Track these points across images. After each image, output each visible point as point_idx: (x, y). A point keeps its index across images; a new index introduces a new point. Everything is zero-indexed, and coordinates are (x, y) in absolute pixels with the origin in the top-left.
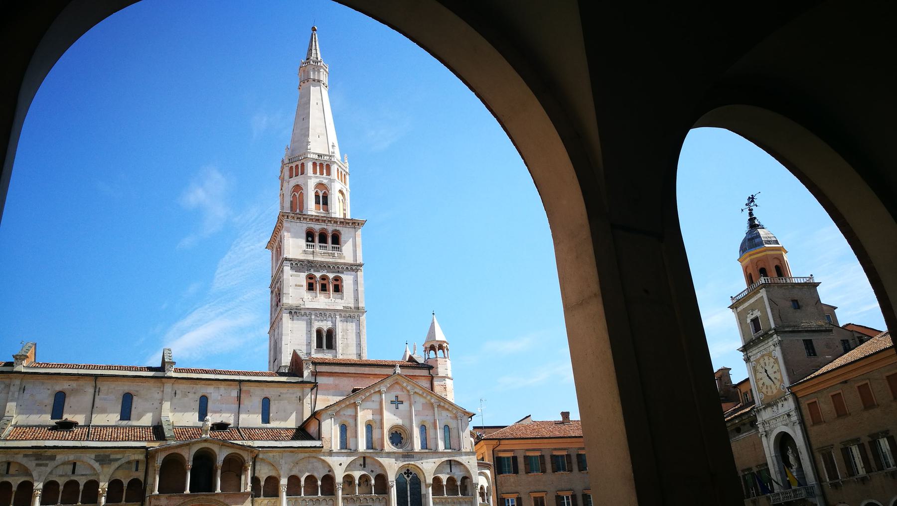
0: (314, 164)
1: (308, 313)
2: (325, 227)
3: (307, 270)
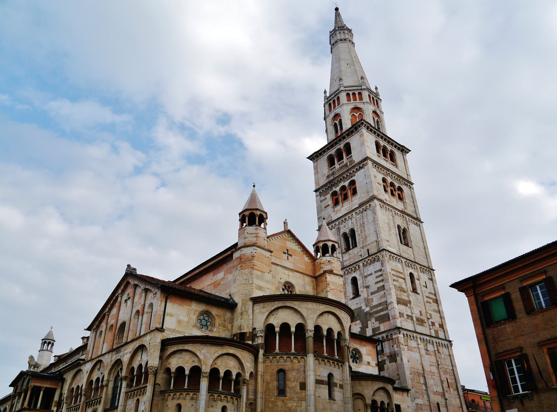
0: (330, 105)
1: (334, 226)
2: (338, 147)
3: (331, 191)
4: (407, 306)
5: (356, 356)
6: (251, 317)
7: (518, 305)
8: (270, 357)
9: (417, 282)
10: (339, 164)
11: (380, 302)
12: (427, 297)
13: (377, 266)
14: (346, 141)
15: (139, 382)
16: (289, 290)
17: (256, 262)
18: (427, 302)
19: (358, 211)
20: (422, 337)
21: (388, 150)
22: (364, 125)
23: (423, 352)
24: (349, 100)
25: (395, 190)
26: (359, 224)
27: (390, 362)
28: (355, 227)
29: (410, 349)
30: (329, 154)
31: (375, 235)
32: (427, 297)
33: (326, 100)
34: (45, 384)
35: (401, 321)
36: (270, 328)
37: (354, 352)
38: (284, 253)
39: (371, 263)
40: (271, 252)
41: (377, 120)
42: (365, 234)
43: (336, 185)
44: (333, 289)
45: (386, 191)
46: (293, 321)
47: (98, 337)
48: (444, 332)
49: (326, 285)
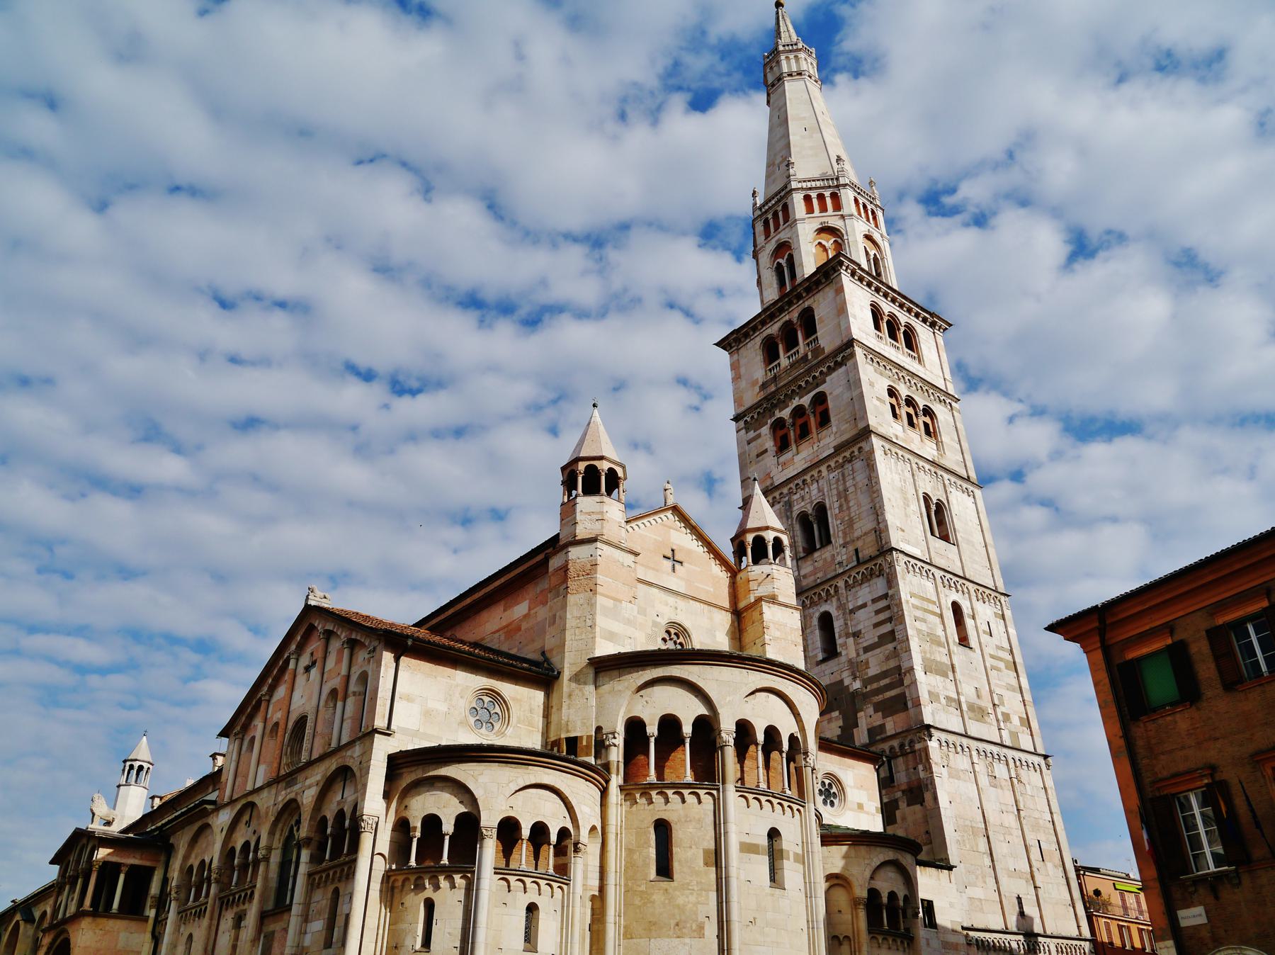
0: (766, 223)
1: (778, 497)
2: (787, 318)
3: (770, 417)
4: (948, 678)
5: (832, 791)
6: (593, 702)
7: (1206, 670)
8: (634, 792)
9: (969, 623)
10: (789, 357)
11: (884, 669)
12: (992, 657)
13: (879, 586)
14: (803, 305)
15: (337, 852)
16: (678, 641)
17: (601, 577)
18: (993, 668)
19: (832, 464)
20: (982, 746)
21: (901, 324)
22: (844, 268)
23: (984, 780)
24: (810, 210)
25: (917, 415)
26: (835, 492)
27: (908, 805)
28: (827, 500)
29: (954, 775)
30: (765, 334)
31: (872, 517)
32: (992, 657)
33: (758, 213)
34: (128, 858)
35: (932, 711)
36: (635, 727)
37: (827, 782)
38: (664, 557)
39: (865, 579)
40: (636, 554)
41: (875, 255)
42: (849, 515)
43: (782, 404)
44: (778, 638)
45: (895, 415)
46: (688, 710)
47: (247, 750)
48: (1032, 735)
49: (761, 629)
